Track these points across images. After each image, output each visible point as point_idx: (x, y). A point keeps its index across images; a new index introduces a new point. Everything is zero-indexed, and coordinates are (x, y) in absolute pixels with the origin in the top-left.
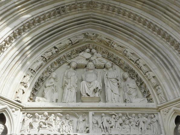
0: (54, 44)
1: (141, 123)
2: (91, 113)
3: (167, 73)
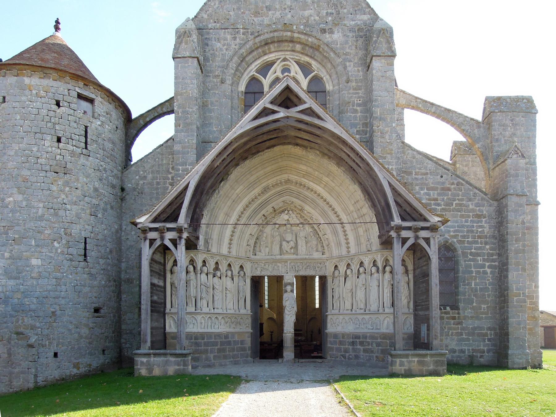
0: (263, 212)
1: (317, 268)
2: (289, 262)
3: (334, 238)
